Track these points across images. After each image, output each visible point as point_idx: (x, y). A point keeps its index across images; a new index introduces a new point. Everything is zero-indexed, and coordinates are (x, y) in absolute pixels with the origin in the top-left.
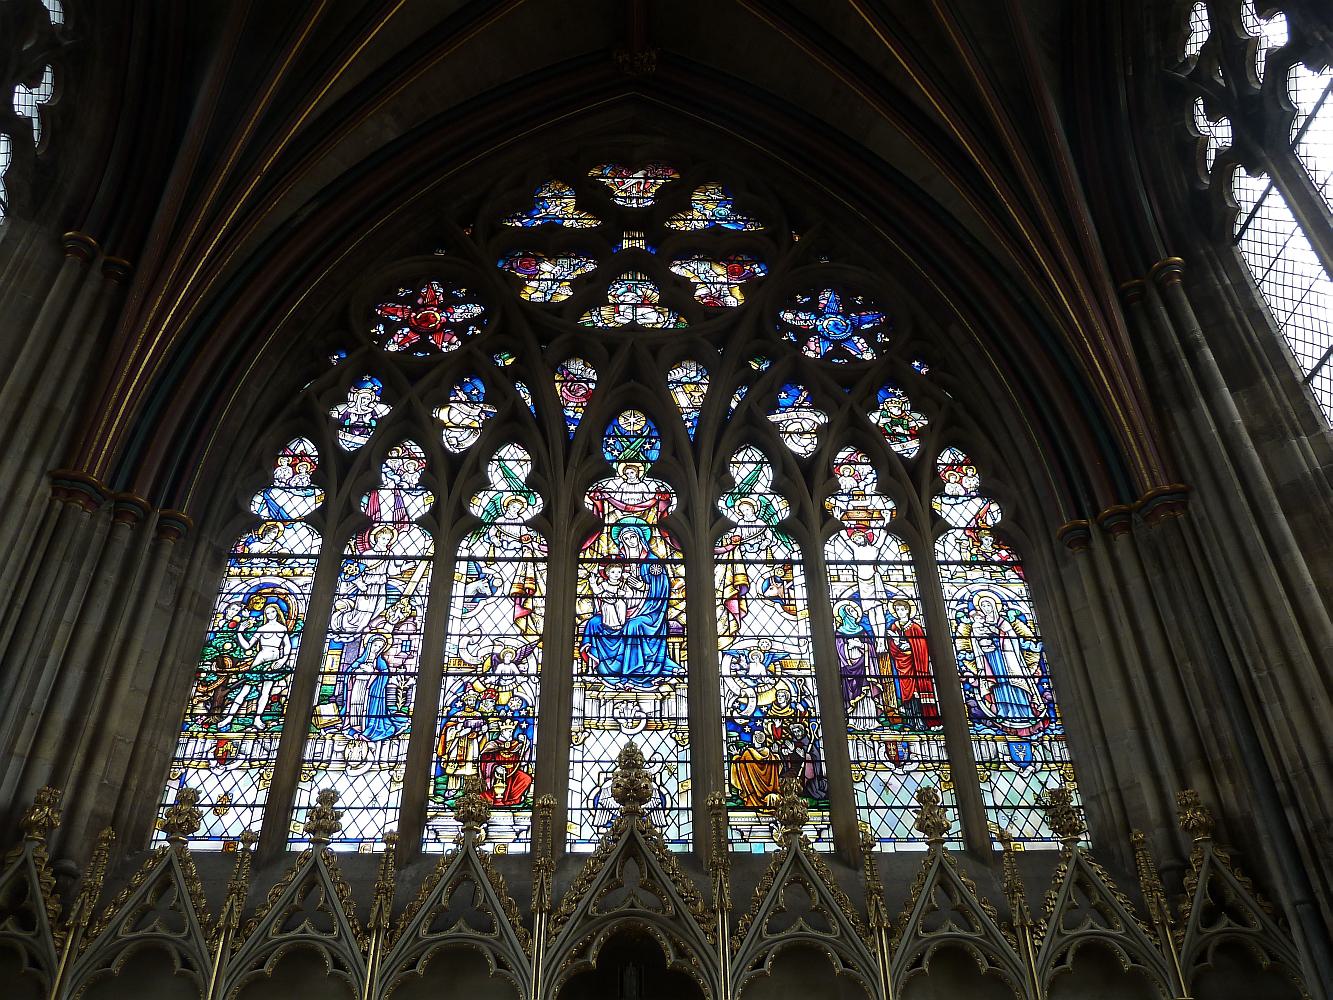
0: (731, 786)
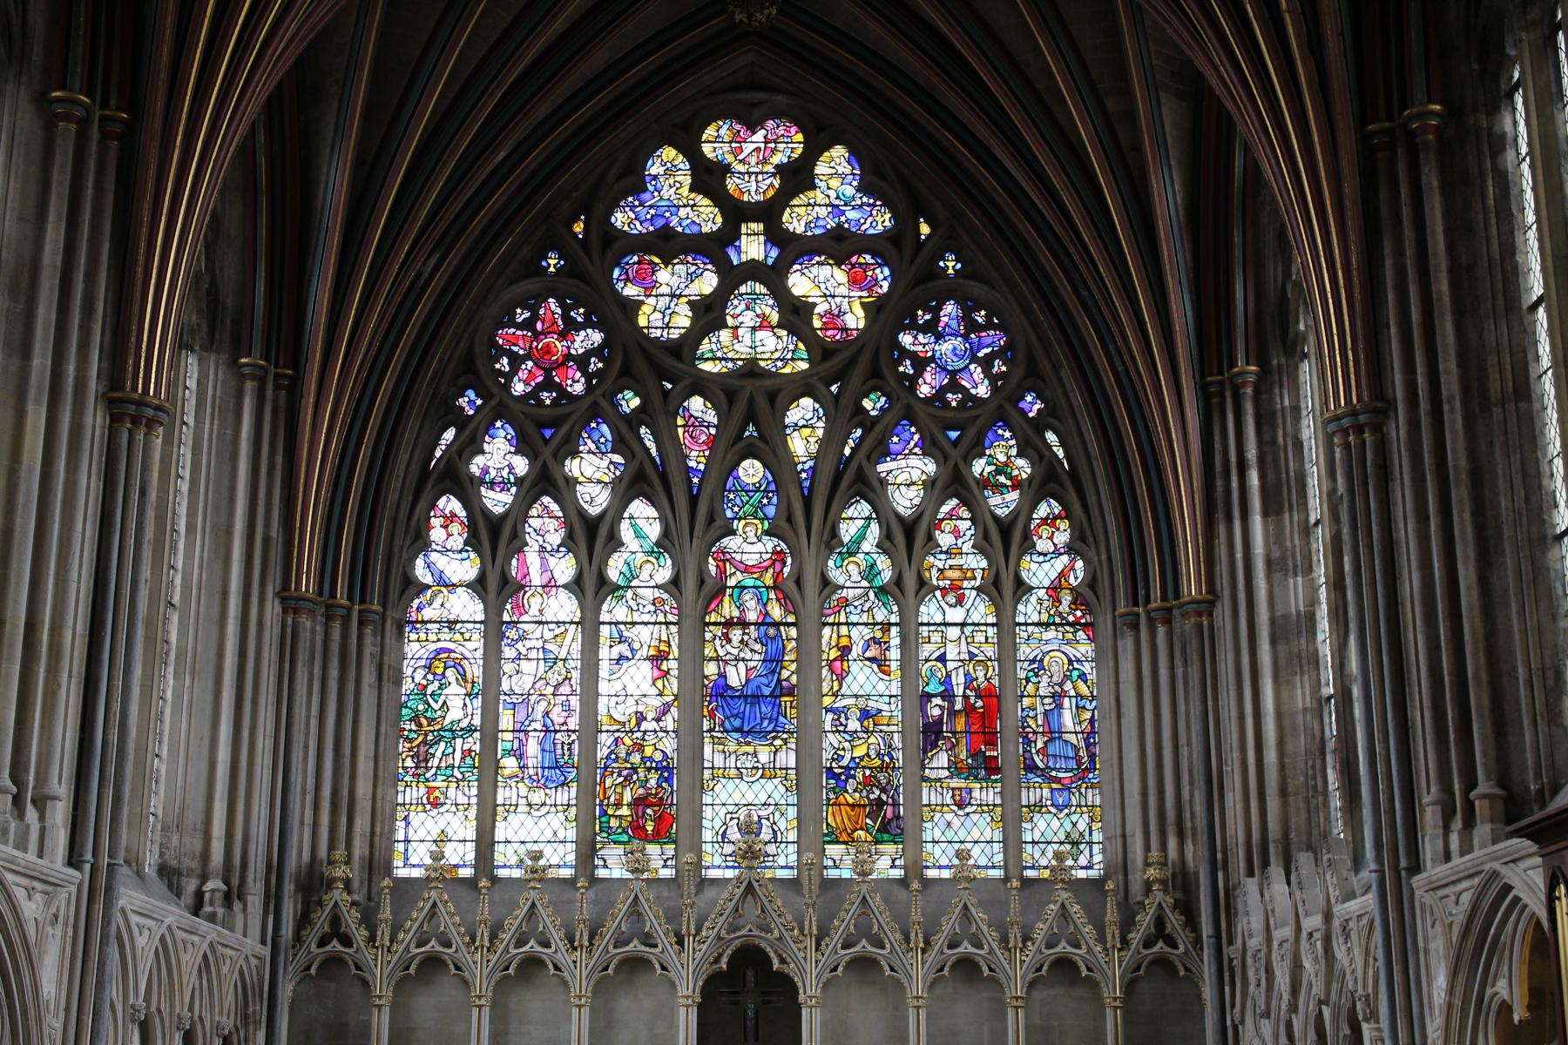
0: (828, 824)
